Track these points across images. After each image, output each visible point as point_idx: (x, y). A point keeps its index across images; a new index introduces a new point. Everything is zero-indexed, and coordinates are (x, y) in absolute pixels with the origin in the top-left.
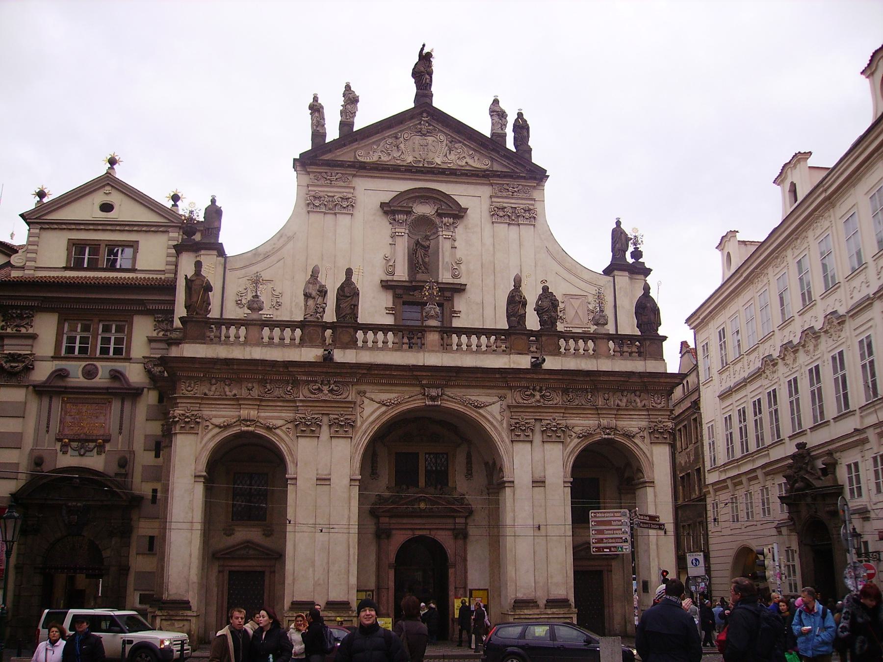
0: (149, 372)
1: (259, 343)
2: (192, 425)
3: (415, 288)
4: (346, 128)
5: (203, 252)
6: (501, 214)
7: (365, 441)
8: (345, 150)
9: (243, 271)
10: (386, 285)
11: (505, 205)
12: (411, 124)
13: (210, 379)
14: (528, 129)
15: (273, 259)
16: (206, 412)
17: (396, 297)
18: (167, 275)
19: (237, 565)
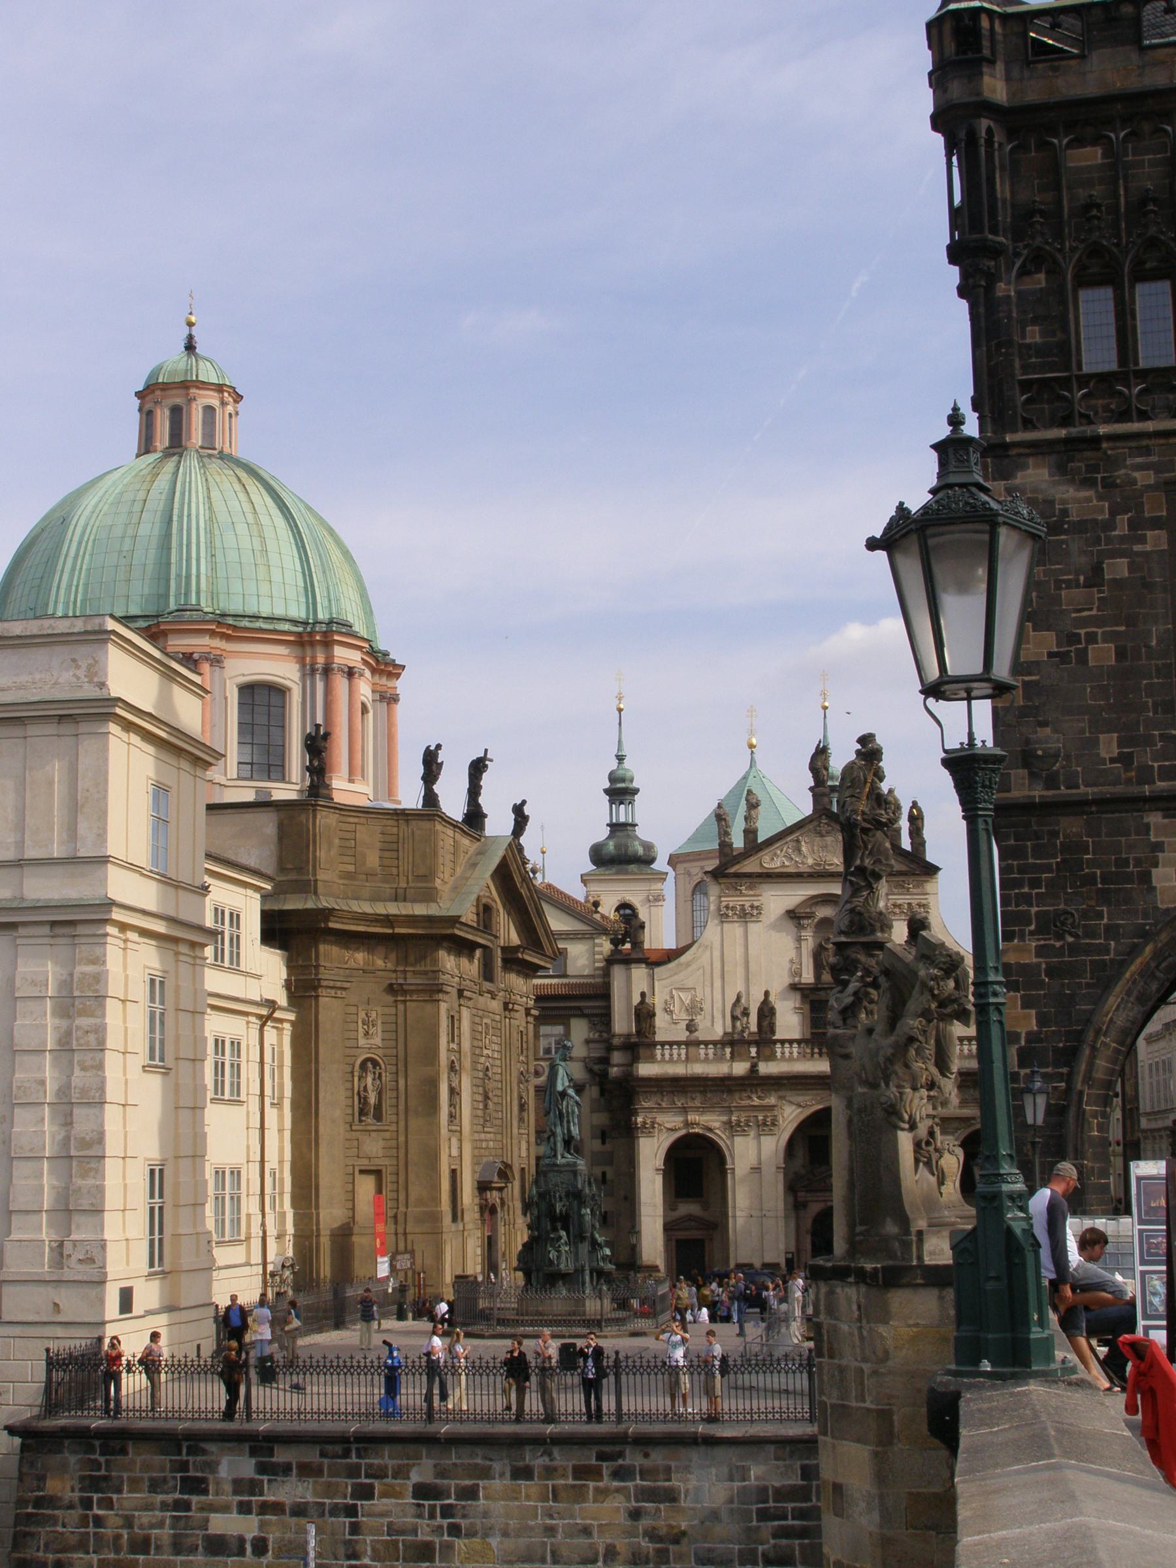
0: (590, 1071)
1: (697, 1060)
2: (650, 1129)
3: (821, 989)
4: (751, 836)
5: (633, 966)
6: (897, 910)
7: (786, 1136)
8: (752, 859)
9: (669, 981)
10: (794, 987)
11: (899, 902)
12: (811, 826)
13: (662, 1093)
14: (922, 819)
15: (694, 966)
16: (658, 1120)
17: (804, 997)
18: (597, 980)
19: (682, 1235)
